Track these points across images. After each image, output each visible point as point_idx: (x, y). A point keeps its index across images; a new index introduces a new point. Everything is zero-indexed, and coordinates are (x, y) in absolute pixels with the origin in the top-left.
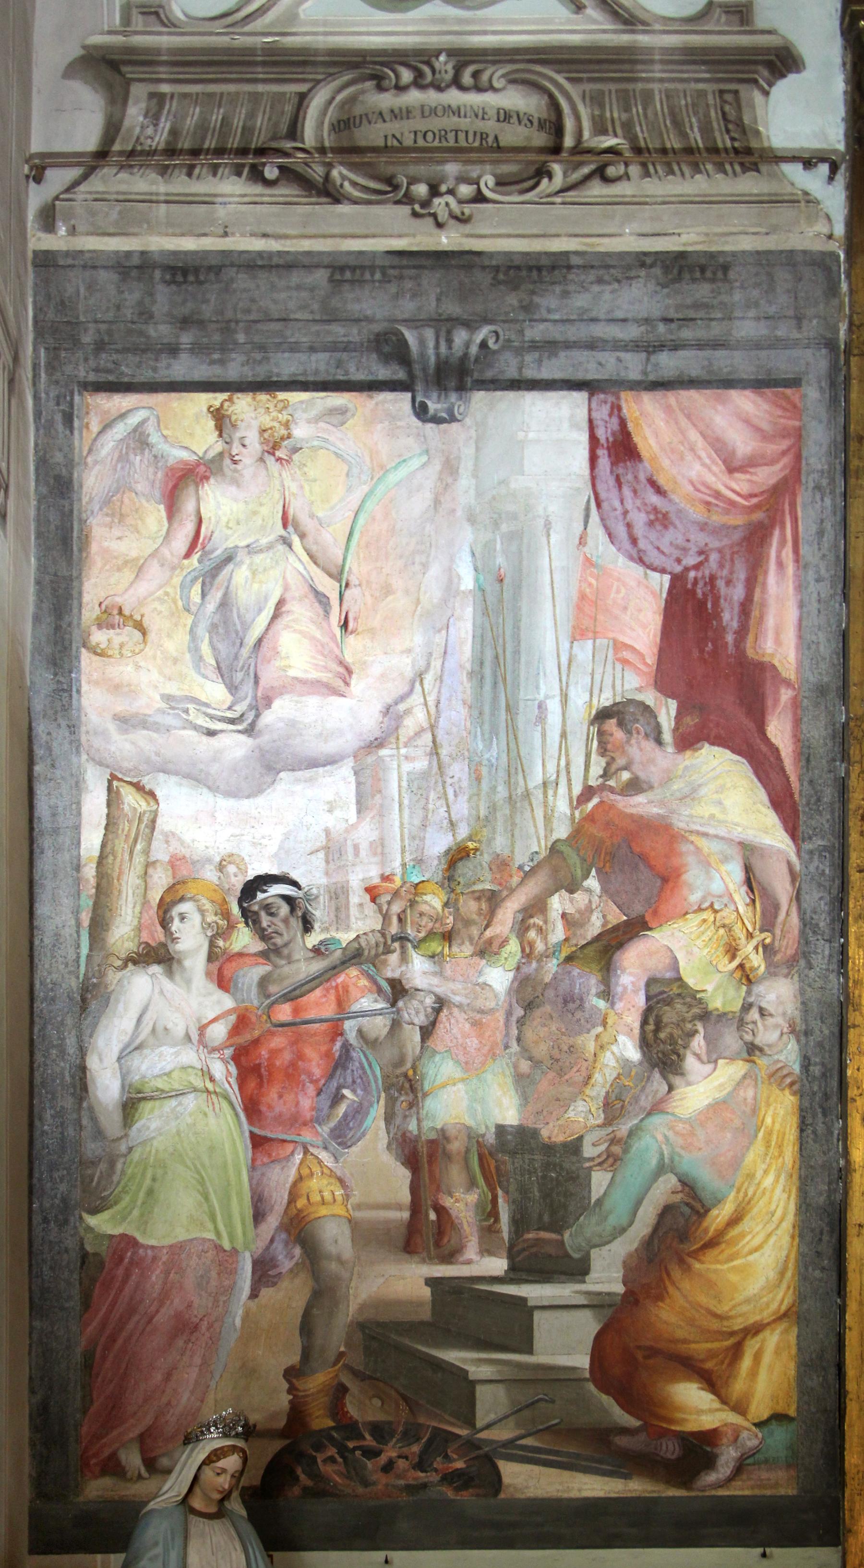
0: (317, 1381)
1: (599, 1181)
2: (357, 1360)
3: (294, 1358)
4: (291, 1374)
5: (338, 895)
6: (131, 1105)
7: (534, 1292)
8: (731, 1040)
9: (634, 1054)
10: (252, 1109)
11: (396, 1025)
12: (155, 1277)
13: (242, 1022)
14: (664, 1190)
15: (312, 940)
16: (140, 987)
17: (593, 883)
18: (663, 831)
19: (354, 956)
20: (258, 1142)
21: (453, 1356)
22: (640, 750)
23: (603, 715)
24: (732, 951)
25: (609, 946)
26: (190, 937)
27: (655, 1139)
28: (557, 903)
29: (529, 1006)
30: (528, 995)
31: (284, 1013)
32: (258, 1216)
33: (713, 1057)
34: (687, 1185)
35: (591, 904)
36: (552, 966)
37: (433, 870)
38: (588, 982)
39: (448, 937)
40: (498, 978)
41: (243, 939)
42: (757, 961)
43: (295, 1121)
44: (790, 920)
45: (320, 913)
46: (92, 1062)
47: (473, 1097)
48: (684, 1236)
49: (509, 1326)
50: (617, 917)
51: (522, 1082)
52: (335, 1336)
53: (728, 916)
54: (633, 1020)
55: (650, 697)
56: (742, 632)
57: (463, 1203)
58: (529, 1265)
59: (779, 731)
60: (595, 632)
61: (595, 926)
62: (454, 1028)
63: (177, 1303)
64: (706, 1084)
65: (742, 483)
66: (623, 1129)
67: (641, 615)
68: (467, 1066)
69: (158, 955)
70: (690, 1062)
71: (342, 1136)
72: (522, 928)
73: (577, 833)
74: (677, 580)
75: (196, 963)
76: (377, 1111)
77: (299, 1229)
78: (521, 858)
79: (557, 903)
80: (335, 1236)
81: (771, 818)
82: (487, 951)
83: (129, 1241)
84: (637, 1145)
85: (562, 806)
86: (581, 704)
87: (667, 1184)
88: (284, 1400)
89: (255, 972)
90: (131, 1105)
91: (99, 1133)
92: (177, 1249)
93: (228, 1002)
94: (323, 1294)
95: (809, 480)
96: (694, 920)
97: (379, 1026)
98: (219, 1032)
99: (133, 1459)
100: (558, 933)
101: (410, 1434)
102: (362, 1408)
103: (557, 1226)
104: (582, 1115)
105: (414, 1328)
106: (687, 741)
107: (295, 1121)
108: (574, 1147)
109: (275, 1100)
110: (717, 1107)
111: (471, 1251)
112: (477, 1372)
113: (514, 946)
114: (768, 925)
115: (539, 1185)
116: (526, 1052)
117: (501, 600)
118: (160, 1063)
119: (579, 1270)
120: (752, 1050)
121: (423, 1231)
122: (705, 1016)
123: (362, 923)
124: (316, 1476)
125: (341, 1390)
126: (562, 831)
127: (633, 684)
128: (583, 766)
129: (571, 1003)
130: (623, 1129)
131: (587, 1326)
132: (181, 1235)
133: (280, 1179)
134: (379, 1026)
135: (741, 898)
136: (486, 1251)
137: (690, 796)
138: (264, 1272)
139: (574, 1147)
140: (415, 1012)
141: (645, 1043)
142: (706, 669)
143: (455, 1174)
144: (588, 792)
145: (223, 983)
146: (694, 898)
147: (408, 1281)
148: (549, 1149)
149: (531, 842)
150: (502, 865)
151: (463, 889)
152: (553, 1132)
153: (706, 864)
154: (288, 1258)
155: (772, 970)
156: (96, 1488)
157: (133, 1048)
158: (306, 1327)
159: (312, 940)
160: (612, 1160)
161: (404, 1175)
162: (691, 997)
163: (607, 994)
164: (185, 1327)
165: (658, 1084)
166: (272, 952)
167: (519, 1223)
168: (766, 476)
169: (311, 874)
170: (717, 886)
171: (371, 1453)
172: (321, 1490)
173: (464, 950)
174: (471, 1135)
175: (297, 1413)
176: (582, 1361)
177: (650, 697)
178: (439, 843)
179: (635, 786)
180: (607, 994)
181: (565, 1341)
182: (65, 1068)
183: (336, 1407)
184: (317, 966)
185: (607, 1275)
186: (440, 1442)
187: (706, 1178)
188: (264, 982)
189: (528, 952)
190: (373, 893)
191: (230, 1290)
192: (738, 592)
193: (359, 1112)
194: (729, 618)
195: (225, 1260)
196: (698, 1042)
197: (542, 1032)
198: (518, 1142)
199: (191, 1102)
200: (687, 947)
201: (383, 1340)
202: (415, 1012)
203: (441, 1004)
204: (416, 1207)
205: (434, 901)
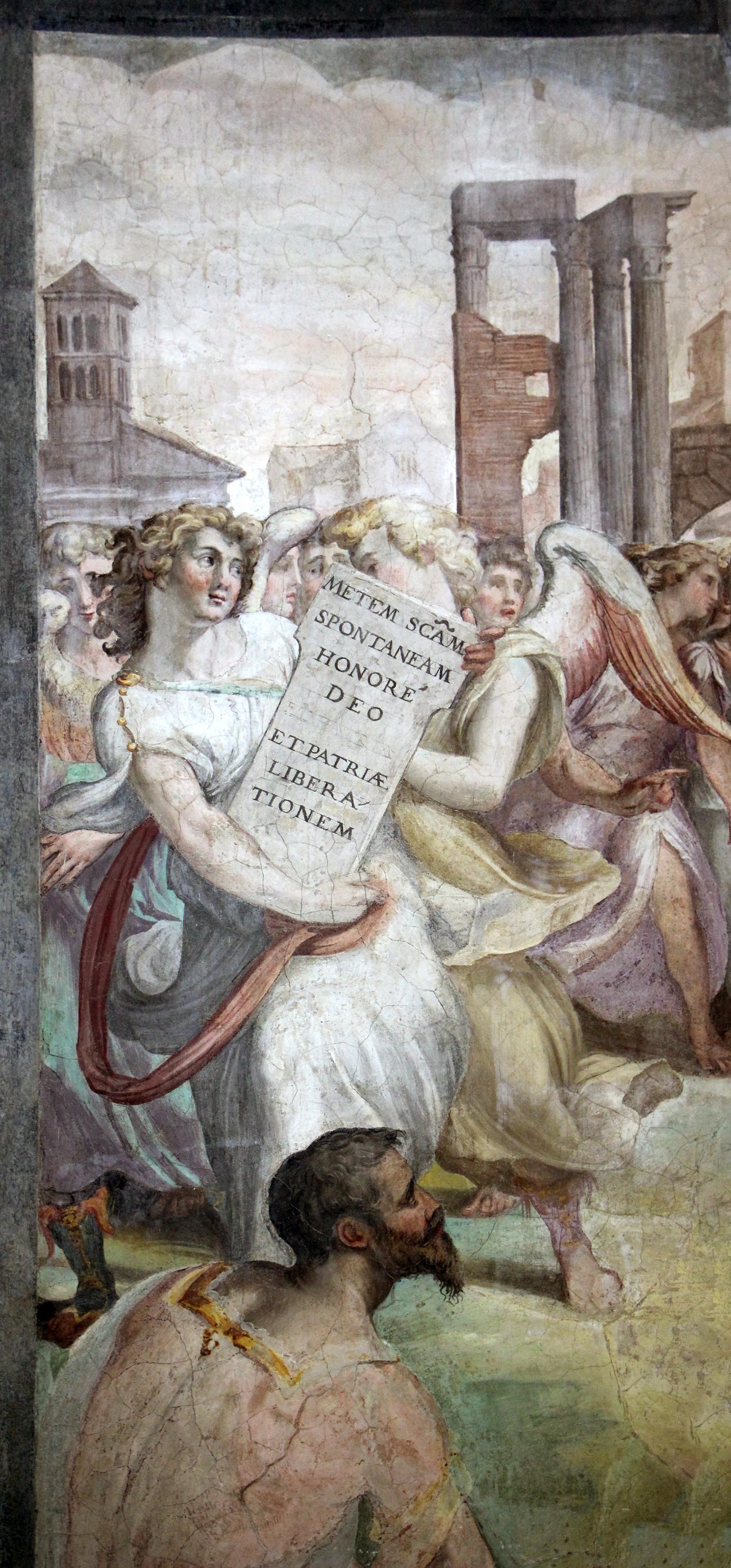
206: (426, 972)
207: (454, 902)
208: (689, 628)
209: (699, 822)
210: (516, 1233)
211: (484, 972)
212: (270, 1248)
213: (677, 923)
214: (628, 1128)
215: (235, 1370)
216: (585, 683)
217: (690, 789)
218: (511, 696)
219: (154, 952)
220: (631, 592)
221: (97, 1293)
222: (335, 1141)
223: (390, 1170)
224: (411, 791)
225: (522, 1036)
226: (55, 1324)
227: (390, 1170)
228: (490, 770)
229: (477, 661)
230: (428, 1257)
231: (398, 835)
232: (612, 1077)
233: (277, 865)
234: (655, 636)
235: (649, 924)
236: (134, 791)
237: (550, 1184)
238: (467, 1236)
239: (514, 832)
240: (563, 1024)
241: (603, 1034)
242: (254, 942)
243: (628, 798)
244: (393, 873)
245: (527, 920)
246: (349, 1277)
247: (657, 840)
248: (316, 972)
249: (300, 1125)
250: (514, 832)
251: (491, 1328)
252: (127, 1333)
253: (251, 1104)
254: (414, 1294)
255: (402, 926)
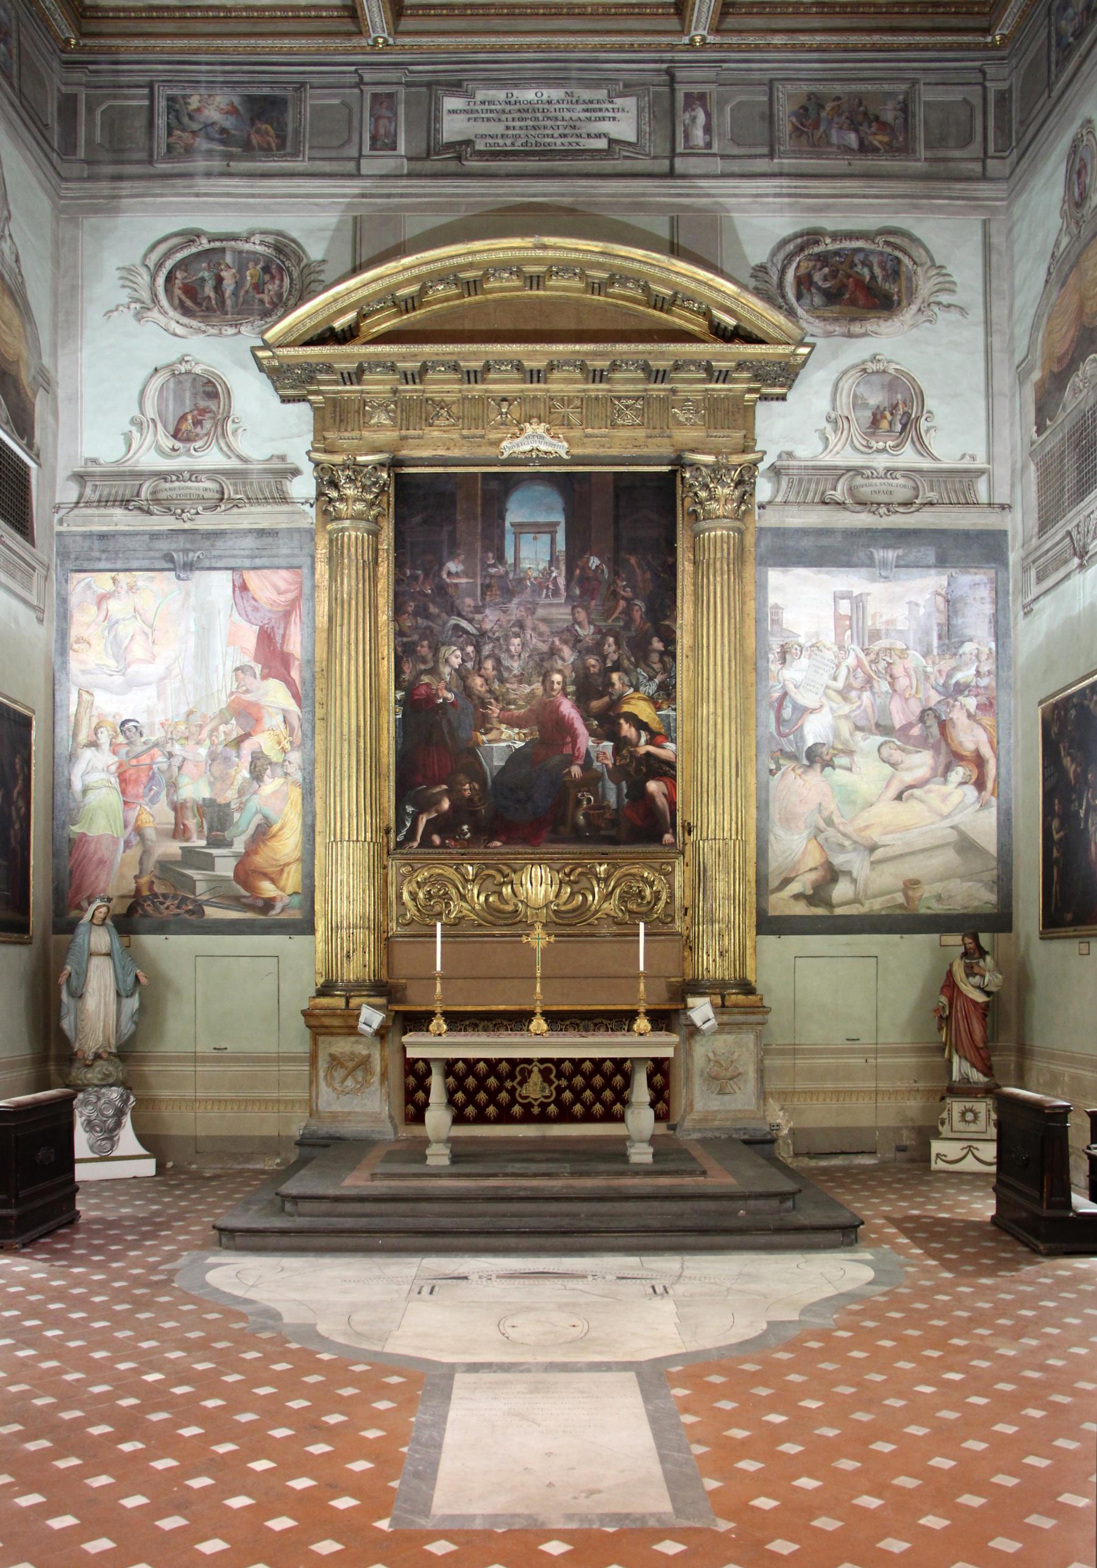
0: (144, 880)
1: (236, 816)
2: (157, 873)
3: (137, 872)
4: (136, 877)
5: (152, 725)
6: (85, 791)
7: (215, 852)
8: (279, 771)
9: (248, 775)
10: (124, 792)
11: (170, 766)
12: (93, 846)
13: (121, 765)
14: (257, 820)
15: (143, 739)
16: (88, 754)
17: (233, 721)
18: (257, 705)
19: (156, 745)
20: (125, 803)
21: (189, 872)
22: (249, 680)
23: (237, 669)
24: (279, 743)
25: (239, 741)
26: (104, 738)
27: (254, 803)
28: (222, 728)
29: (213, 760)
30: (213, 757)
31: (134, 762)
32: (126, 827)
33: (273, 777)
34: (265, 817)
35: (234, 729)
36: (220, 748)
37: (182, 717)
38: (233, 753)
39: (187, 738)
40: (203, 751)
41: (121, 739)
42: (288, 746)
43: (137, 796)
44: (298, 733)
45: (145, 731)
46: (73, 778)
47: (195, 789)
48: (264, 834)
49: (207, 863)
50: (241, 732)
51: (211, 784)
52: (150, 865)
53: (278, 732)
54: (247, 765)
55: (252, 664)
56: (283, 644)
57: (192, 823)
58: (214, 843)
59: (295, 674)
60: (234, 642)
61: (234, 735)
62: (188, 767)
63: (99, 855)
64: (271, 785)
65: (283, 598)
66: (244, 799)
67: (249, 637)
68: (193, 779)
69: (94, 744)
70: (266, 778)
71: (153, 801)
72: (210, 736)
73: (228, 707)
74: (261, 628)
75: (106, 747)
76: (164, 793)
77: (139, 831)
78: (210, 714)
79: (222, 728)
80: (150, 833)
81: (292, 701)
82: (198, 743)
83: (84, 835)
84: (249, 805)
85: (224, 698)
86: (230, 666)
87: (259, 816)
88: (134, 886)
89: (123, 750)
90: (85, 791)
91: (75, 800)
92: (100, 837)
93: (116, 759)
94: (146, 852)
95: (304, 597)
96: (266, 734)
97: (164, 766)
98: (113, 768)
99: (85, 904)
100: (222, 737)
101: (175, 897)
102: (159, 889)
103: (223, 830)
104: (230, 795)
105: (175, 863)
106: (264, 677)
107: (137, 796)
108: (228, 805)
109: (131, 790)
110: (275, 792)
111: (195, 838)
112: (196, 877)
113: (208, 742)
114: (291, 734)
115: (217, 819)
116: (212, 775)
117: (204, 632)
118: (93, 778)
119: (230, 844)
120: (286, 774)
121: (179, 832)
122: (271, 763)
123: (158, 734)
124: (144, 910)
125: (152, 883)
126: (223, 706)
127: (247, 660)
128: (231, 685)
129: (227, 759)
130: (244, 799)
131: (233, 862)
132: (101, 832)
133: (132, 815)
134: (164, 766)
135: (282, 726)
136: (199, 838)
137: (266, 694)
138: (127, 844)
139: (228, 805)
140: (176, 762)
141: (251, 772)
142: (272, 656)
143: (189, 813)
144: (232, 693)
145: (114, 753)
146: (267, 726)
147: (173, 848)
148: (219, 805)
149: (214, 709)
150: (204, 716)
151: (192, 724)
152: (221, 800)
153: (270, 716)
154: (135, 840)
155: (293, 749)
156: (74, 913)
157: (86, 773)
158: (141, 862)
159: (143, 739)
160: (241, 809)
161: (172, 814)
162: (266, 757)
163: (238, 756)
164: (102, 862)
165: (255, 785)
166: (130, 743)
167: (210, 829)
168: (290, 596)
169: (143, 719)
170: (274, 723)
171: (162, 903)
172: (146, 915)
173: (192, 743)
174: (194, 801)
175: (138, 890)
176: (231, 874)
177: (252, 664)
178: (184, 709)
179: (247, 691)
180: (238, 756)
181: (225, 868)
182: (63, 780)
183: (151, 889)
184: (145, 748)
185: (239, 847)
186: (184, 900)
187: (272, 815)
188: (127, 753)
189: (212, 743)
190: (162, 725)
191: (116, 850)
192: (281, 631)
193: (157, 794)
194: (278, 639)
195: (115, 841)
196: (268, 772)
197: (217, 768)
198: (210, 803)
199: (104, 790)
200: (265, 742)
201: (165, 867)
202: (176, 762)
203: (184, 760)
204: (176, 824)
205: (182, 727)
206: (830, 717)
207: (834, 705)
208: (871, 661)
209: (873, 694)
210: (843, 760)
211: (840, 717)
212: (805, 762)
213: (870, 710)
214: (862, 744)
215: (799, 781)
216: (855, 670)
217: (871, 688)
218: (843, 672)
219: (787, 713)
220: (862, 655)
221: (778, 768)
222: (815, 744)
223: (824, 750)
224: (827, 687)
225: (845, 728)
226: (772, 772)
227: (824, 750)
228: (840, 684)
229: (838, 666)
230: (829, 764)
231: (825, 694)
232: (859, 735)
233: (806, 699)
234: (866, 663)
235: (865, 711)
236: (784, 687)
237: (850, 753)
238: (836, 761)
239: (844, 694)
240: (852, 727)
241: (858, 728)
242: (802, 711)
243: (862, 689)
244: (824, 700)
245: (846, 709)
246: (818, 767)
247: (866, 696)
248: (812, 717)
249: (810, 742)
250: (844, 694)
251: (839, 776)
252: (783, 774)
253: (802, 738)
254: (828, 770)
255: (826, 710)
